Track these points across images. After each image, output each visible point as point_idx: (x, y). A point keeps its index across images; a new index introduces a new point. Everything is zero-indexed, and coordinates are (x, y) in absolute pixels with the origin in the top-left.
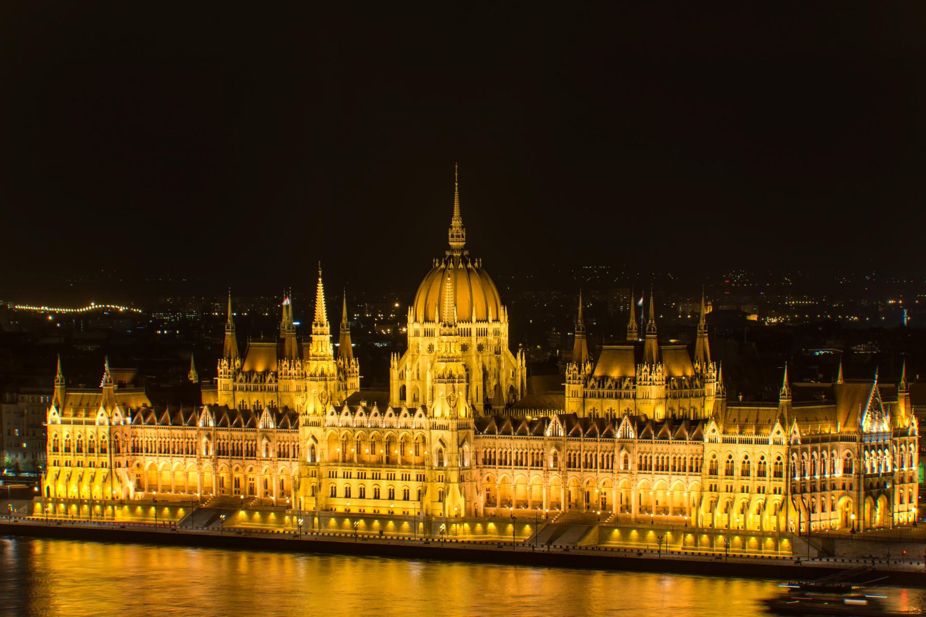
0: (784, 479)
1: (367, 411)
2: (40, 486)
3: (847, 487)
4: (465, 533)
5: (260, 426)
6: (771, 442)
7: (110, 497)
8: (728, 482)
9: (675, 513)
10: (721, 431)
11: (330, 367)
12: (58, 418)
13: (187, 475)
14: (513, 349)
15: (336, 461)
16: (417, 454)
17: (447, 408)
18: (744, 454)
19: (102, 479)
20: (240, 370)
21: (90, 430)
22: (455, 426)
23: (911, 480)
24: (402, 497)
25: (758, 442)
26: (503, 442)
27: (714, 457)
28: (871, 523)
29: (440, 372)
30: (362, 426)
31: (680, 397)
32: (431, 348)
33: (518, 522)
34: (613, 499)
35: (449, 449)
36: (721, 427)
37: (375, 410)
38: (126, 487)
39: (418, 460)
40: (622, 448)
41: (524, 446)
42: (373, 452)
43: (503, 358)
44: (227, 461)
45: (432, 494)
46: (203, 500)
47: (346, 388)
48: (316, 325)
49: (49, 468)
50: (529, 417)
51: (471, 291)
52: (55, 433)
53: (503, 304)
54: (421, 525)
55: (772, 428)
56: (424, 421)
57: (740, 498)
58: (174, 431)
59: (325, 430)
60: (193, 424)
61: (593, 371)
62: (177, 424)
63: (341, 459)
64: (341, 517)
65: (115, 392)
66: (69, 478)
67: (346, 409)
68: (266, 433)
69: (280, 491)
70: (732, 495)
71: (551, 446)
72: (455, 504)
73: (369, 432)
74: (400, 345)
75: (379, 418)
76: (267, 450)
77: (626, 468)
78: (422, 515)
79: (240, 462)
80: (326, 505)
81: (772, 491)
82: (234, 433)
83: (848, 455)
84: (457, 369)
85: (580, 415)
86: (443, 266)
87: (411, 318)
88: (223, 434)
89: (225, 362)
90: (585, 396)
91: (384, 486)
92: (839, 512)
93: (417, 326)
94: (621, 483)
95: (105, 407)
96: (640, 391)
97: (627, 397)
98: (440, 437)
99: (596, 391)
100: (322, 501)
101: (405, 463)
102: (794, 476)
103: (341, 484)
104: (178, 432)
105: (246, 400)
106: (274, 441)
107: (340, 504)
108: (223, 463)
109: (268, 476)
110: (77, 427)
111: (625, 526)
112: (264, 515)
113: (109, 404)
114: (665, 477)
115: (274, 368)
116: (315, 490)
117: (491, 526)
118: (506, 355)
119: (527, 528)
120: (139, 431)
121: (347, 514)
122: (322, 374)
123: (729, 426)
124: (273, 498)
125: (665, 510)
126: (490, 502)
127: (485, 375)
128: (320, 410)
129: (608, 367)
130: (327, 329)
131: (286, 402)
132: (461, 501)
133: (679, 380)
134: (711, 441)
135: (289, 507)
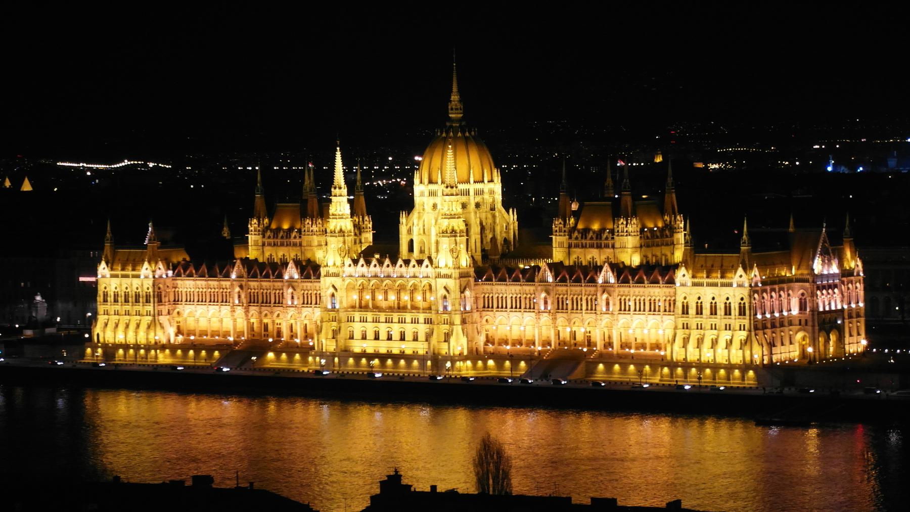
0: (747, 317)
1: (381, 262)
2: (90, 334)
3: (803, 322)
4: (467, 370)
5: (286, 277)
6: (735, 285)
7: (153, 342)
8: (698, 320)
9: (652, 349)
10: (690, 276)
11: (347, 224)
13: (221, 321)
14: (506, 205)
15: (353, 307)
16: (425, 300)
17: (452, 259)
18: (712, 296)
19: (146, 326)
20: (268, 228)
21: (136, 282)
22: (457, 276)
23: (858, 316)
24: (411, 338)
25: (723, 285)
26: (499, 287)
27: (685, 298)
28: (826, 355)
29: (444, 228)
30: (376, 276)
31: (653, 245)
32: (435, 206)
33: (515, 359)
34: (598, 337)
35: (453, 295)
36: (690, 272)
37: (387, 262)
38: (168, 333)
39: (425, 305)
41: (518, 291)
42: (386, 299)
43: (497, 214)
45: (438, 335)
46: (236, 343)
47: (361, 242)
48: (335, 188)
49: (99, 317)
50: (521, 266)
51: (469, 156)
52: (104, 285)
53: (497, 166)
54: (429, 363)
55: (735, 273)
56: (430, 271)
57: (710, 335)
58: (210, 282)
59: (343, 280)
60: (227, 276)
61: (576, 224)
62: (212, 275)
63: (357, 305)
64: (358, 357)
65: (158, 248)
66: (117, 326)
67: (362, 261)
68: (291, 283)
69: (303, 334)
70: (702, 332)
71: (542, 291)
72: (459, 344)
73: (382, 281)
74: (408, 205)
75: (391, 269)
76: (293, 298)
77: (608, 309)
78: (430, 354)
79: (269, 309)
80: (346, 347)
81: (738, 328)
82: (264, 284)
83: (803, 294)
84: (459, 224)
85: (567, 263)
86: (444, 135)
87: (416, 180)
88: (253, 284)
89: (255, 221)
90: (570, 246)
91: (396, 329)
92: (797, 345)
94: (604, 322)
95: (149, 262)
96: (618, 241)
97: (607, 246)
99: (579, 242)
100: (342, 343)
101: (415, 308)
102: (756, 314)
103: (357, 328)
104: (213, 283)
105: (274, 254)
106: (298, 290)
107: (357, 346)
108: (253, 310)
109: (293, 321)
110: (125, 280)
111: (609, 360)
112: (291, 356)
113: (153, 260)
114: (642, 317)
115: (298, 226)
116: (335, 333)
117: (491, 363)
118: (500, 212)
119: (523, 364)
120: (179, 282)
121: (364, 354)
122: (341, 231)
123: (697, 272)
124: (298, 341)
125: (643, 346)
126: (488, 341)
127: (483, 228)
128: (339, 263)
129: (589, 221)
130: (344, 191)
131: (309, 255)
132: (464, 341)
133: (651, 230)
134: (682, 285)
135: (313, 348)
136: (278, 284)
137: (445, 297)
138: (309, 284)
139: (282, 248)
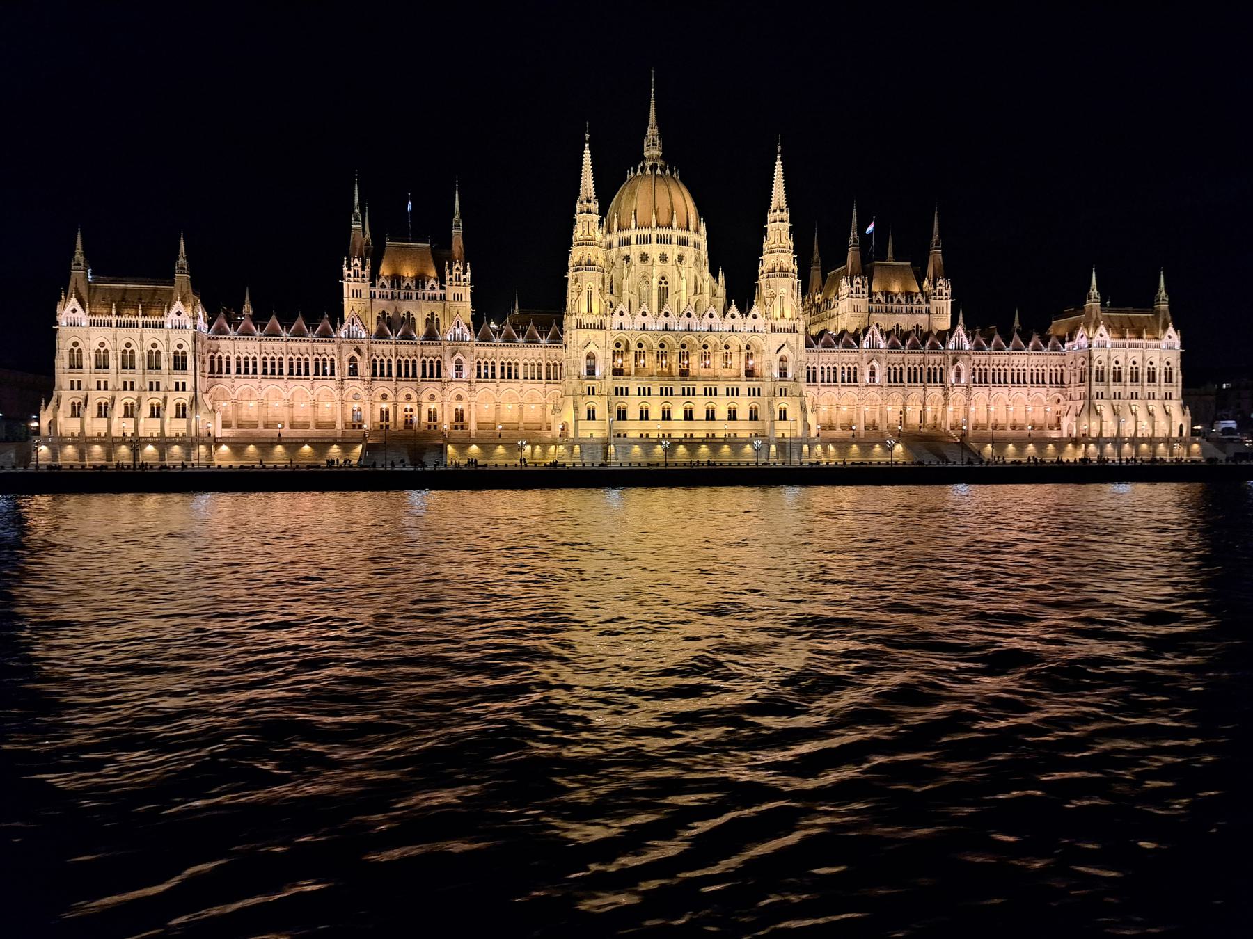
12: (82, 317)
20: (375, 275)
21: (151, 335)
32: (663, 258)
40: (955, 361)
41: (832, 360)
44: (391, 385)
48: (589, 201)
54: (773, 448)
76: (459, 368)
77: (958, 380)
79: (413, 385)
82: (400, 347)
86: (658, 171)
90: (870, 311)
93: (646, 232)
95: (183, 301)
96: (934, 304)
97: (920, 312)
103: (633, 405)
107: (633, 428)
108: (381, 387)
120: (221, 343)
130: (594, 207)
136: (431, 349)
138: (490, 350)
139: (408, 302)
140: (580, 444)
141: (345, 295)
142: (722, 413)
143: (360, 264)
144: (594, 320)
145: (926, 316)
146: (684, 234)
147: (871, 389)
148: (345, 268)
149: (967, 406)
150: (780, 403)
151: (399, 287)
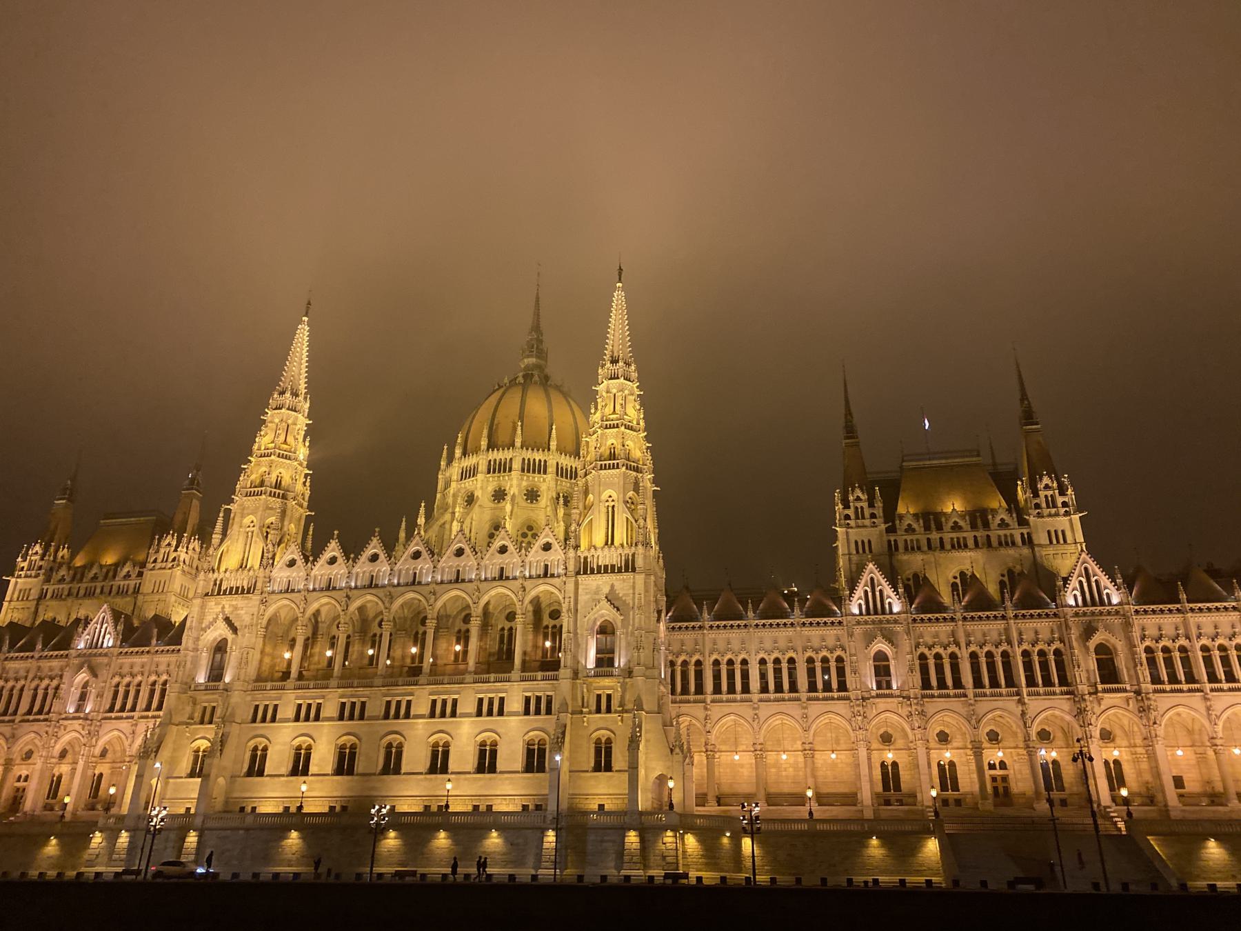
24: (471, 762)
26: (722, 635)
30: (372, 585)
32: (499, 495)
35: (637, 618)
40: (1089, 631)
41: (782, 644)
48: (282, 393)
54: (551, 836)
56: (556, 557)
71: (869, 639)
73: (392, 598)
76: (83, 697)
90: (892, 548)
96: (1040, 526)
97: (1009, 543)
98: (606, 590)
103: (282, 740)
106: (104, 674)
107: (271, 796)
117: (747, 843)
122: (278, 485)
128: (254, 561)
137: (606, 630)
139: (87, 602)
140: (133, 831)
141: (7, 598)
142: (463, 755)
143: (40, 552)
144: (242, 580)
145: (1026, 551)
146: (538, 456)
147: (882, 704)
148: (19, 559)
149: (1149, 741)
150: (598, 725)
151: (81, 580)
